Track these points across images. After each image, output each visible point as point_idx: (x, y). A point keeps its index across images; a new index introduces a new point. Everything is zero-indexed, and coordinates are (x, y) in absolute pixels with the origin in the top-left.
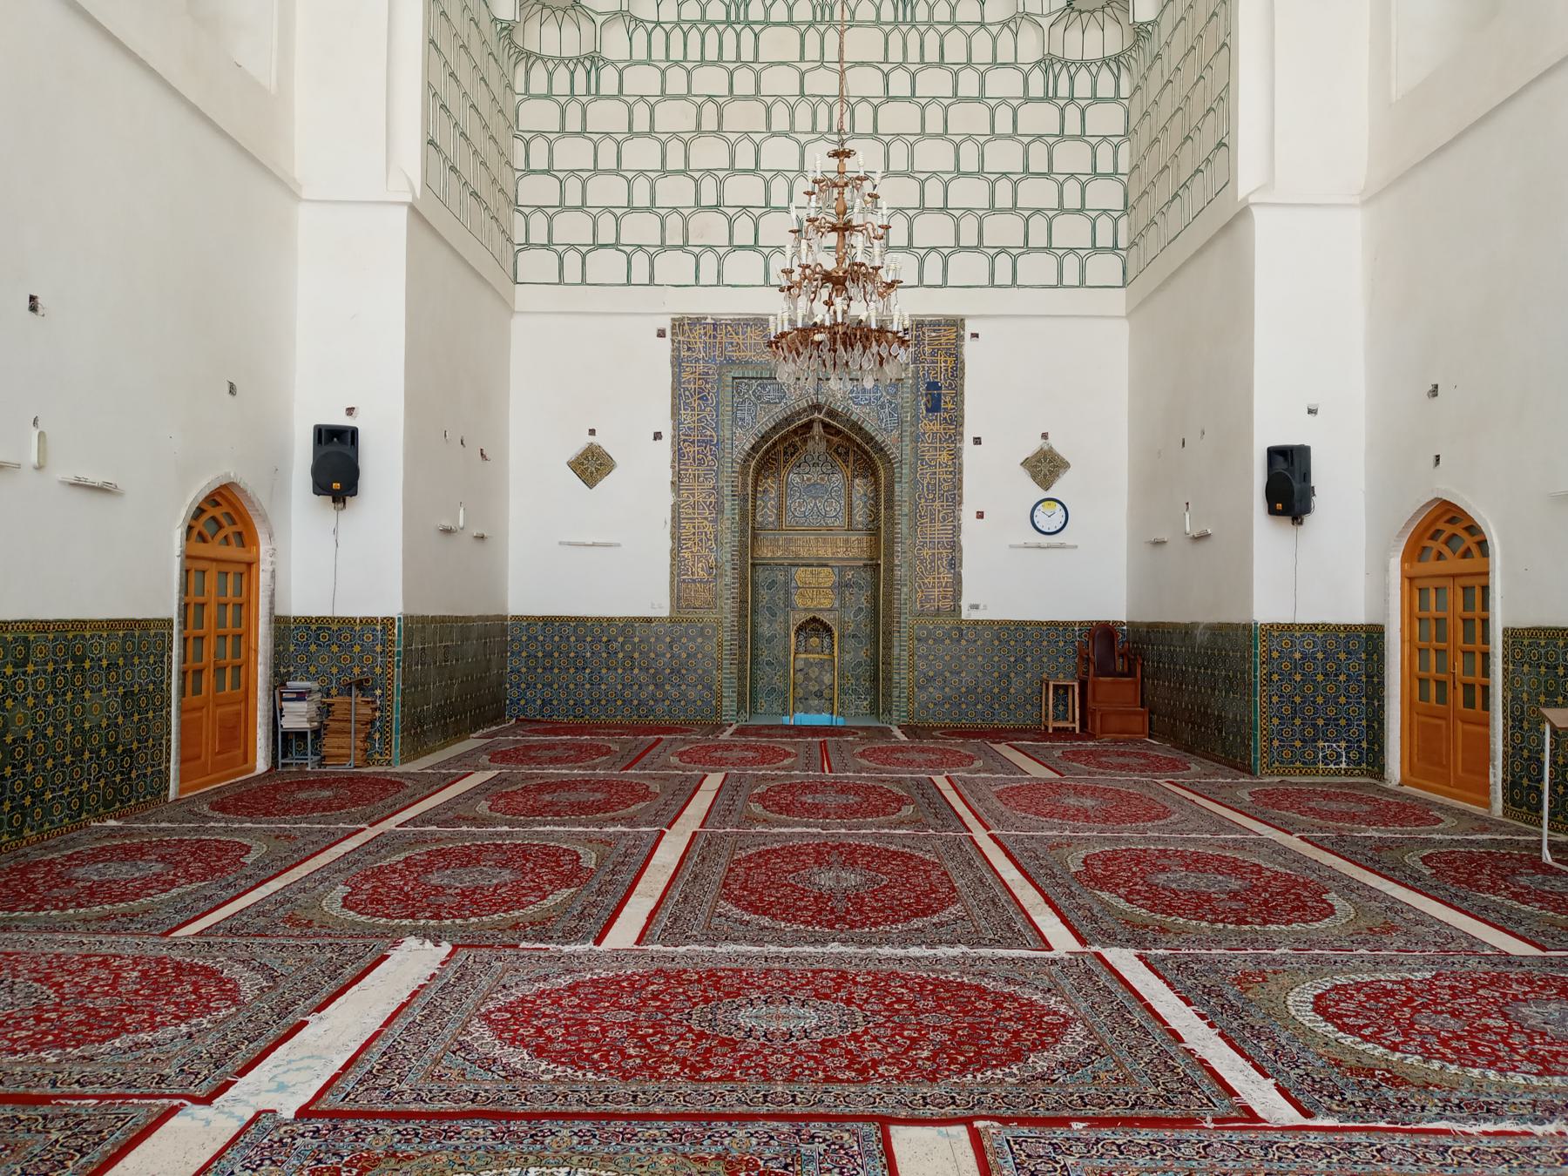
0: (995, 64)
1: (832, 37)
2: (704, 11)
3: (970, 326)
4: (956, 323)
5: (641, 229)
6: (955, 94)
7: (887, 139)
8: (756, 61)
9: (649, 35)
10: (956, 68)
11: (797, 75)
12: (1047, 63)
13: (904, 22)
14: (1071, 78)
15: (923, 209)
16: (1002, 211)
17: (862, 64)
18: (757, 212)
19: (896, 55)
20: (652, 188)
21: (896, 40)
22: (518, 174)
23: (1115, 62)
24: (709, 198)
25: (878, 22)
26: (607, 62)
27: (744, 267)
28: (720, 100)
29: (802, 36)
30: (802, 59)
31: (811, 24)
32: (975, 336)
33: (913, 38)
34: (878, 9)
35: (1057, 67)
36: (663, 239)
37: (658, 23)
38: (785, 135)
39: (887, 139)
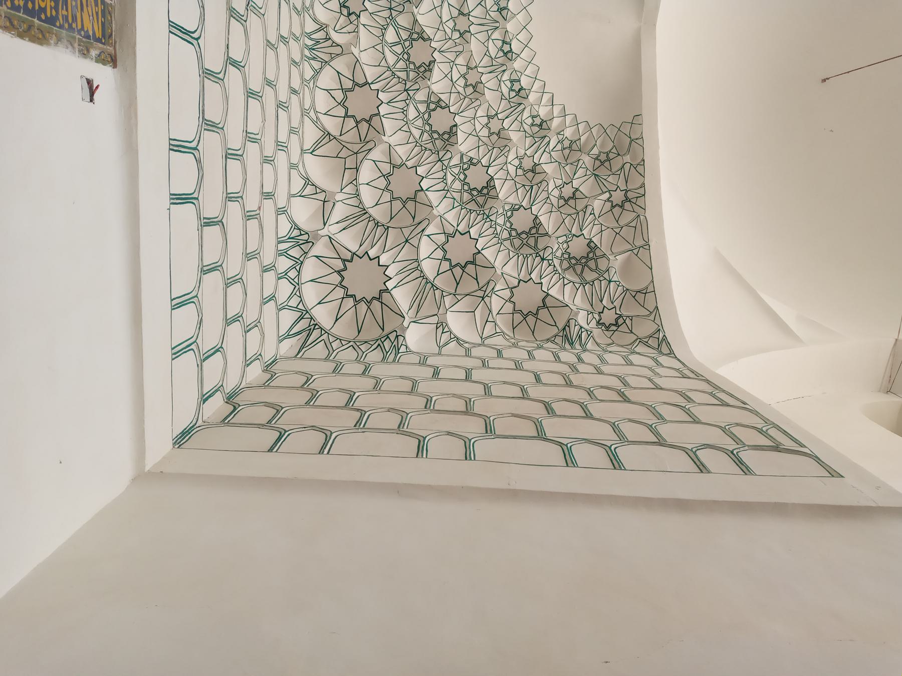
3: (103, 75)
32: (92, 89)
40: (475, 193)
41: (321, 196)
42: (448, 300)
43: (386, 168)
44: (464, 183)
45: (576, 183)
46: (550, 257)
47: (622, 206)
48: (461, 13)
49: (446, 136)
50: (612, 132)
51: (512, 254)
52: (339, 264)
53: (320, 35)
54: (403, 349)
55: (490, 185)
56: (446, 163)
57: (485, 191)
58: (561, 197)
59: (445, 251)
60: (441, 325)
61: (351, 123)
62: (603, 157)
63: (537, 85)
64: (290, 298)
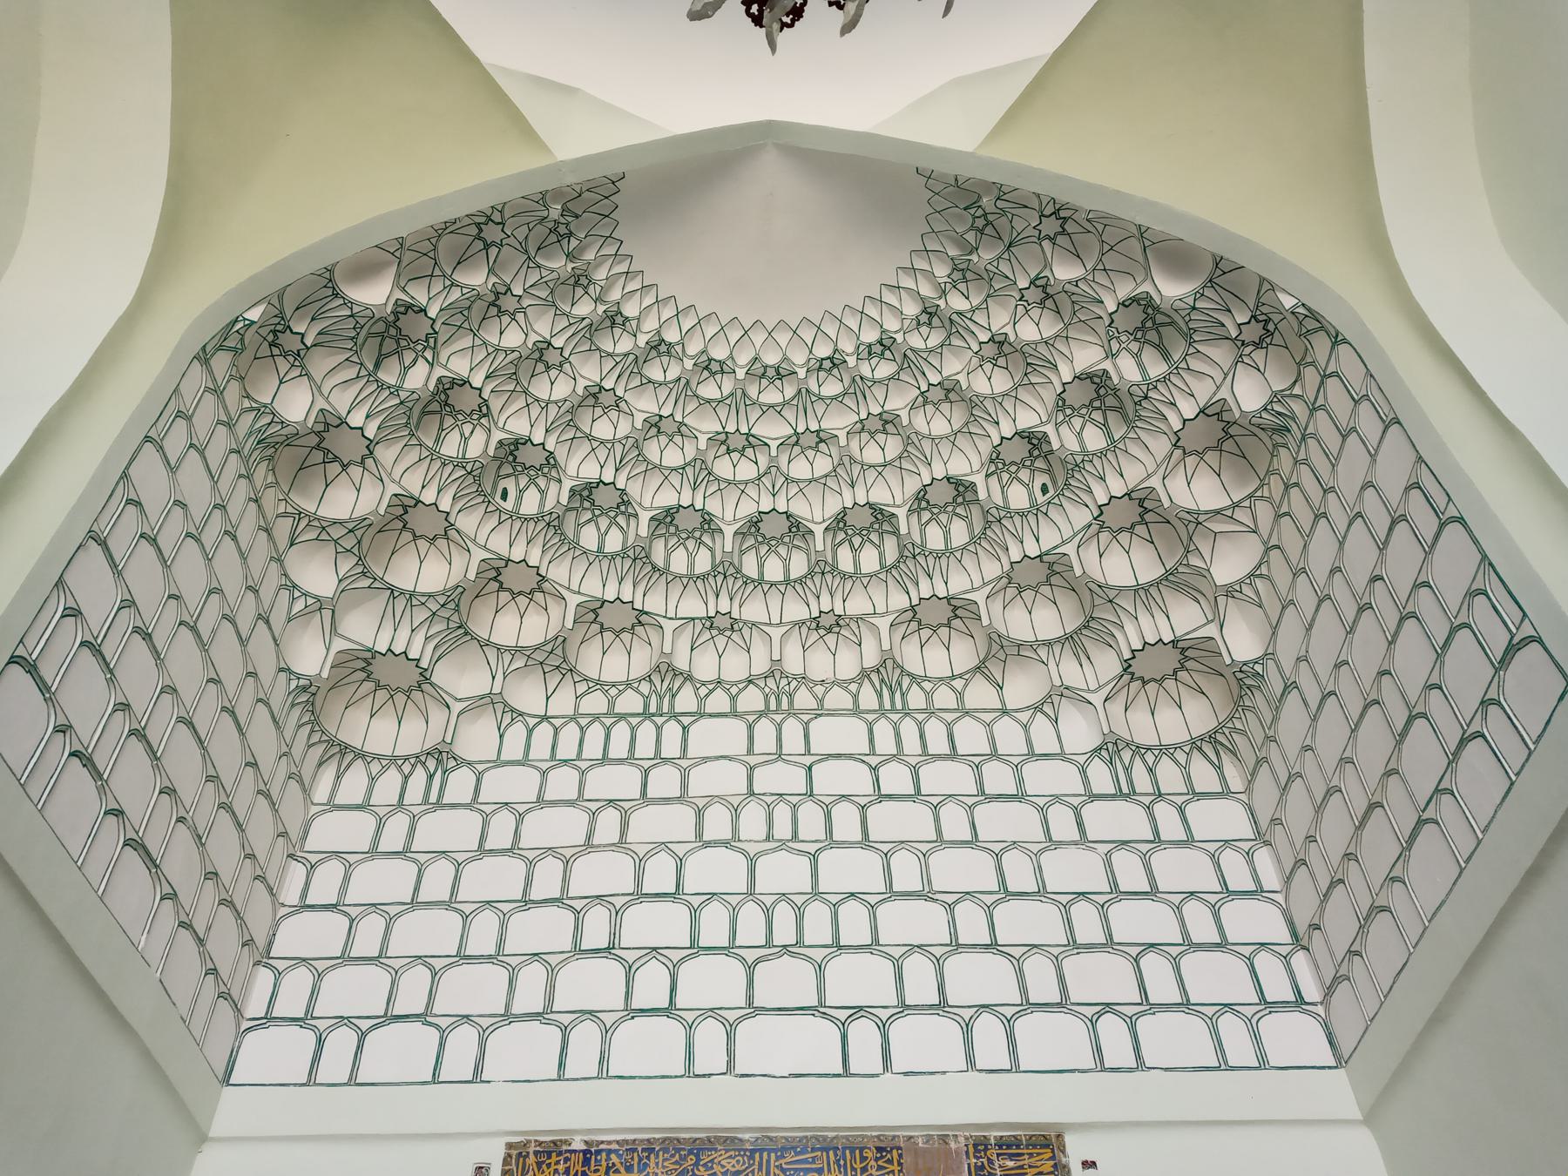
0: (1032, 755)
1: (792, 729)
2: (612, 703)
4: (1047, 1142)
5: (477, 989)
6: (981, 791)
7: (885, 847)
8: (684, 756)
9: (530, 732)
10: (977, 760)
11: (743, 771)
12: (1111, 748)
13: (893, 709)
14: (1151, 770)
15: (956, 946)
16: (1090, 947)
17: (838, 756)
18: (675, 956)
19: (885, 744)
20: (503, 926)
21: (883, 730)
22: (282, 911)
23: (1212, 743)
24: (595, 936)
25: (856, 711)
26: (461, 762)
27: (648, 1045)
28: (626, 805)
29: (750, 728)
30: (750, 751)
31: (762, 714)
32: (1089, 1165)
33: (909, 728)
34: (855, 697)
35: (1126, 755)
36: (508, 1006)
37: (545, 718)
38: (725, 844)
39: (885, 847)
40: (1036, 453)
41: (1056, 699)
42: (1195, 561)
43: (1011, 592)
44: (1021, 465)
45: (1023, 283)
46: (1144, 388)
47: (1065, 219)
48: (797, 443)
49: (961, 489)
50: (941, 203)
51: (1132, 435)
52: (1136, 685)
53: (874, 677)
54: (1258, 668)
55: (1027, 436)
56: (1003, 514)
57: (1035, 441)
58: (1042, 303)
59: (1121, 530)
60: (1230, 592)
61: (956, 623)
62: (980, 223)
63: (873, 311)
64: (1176, 762)
